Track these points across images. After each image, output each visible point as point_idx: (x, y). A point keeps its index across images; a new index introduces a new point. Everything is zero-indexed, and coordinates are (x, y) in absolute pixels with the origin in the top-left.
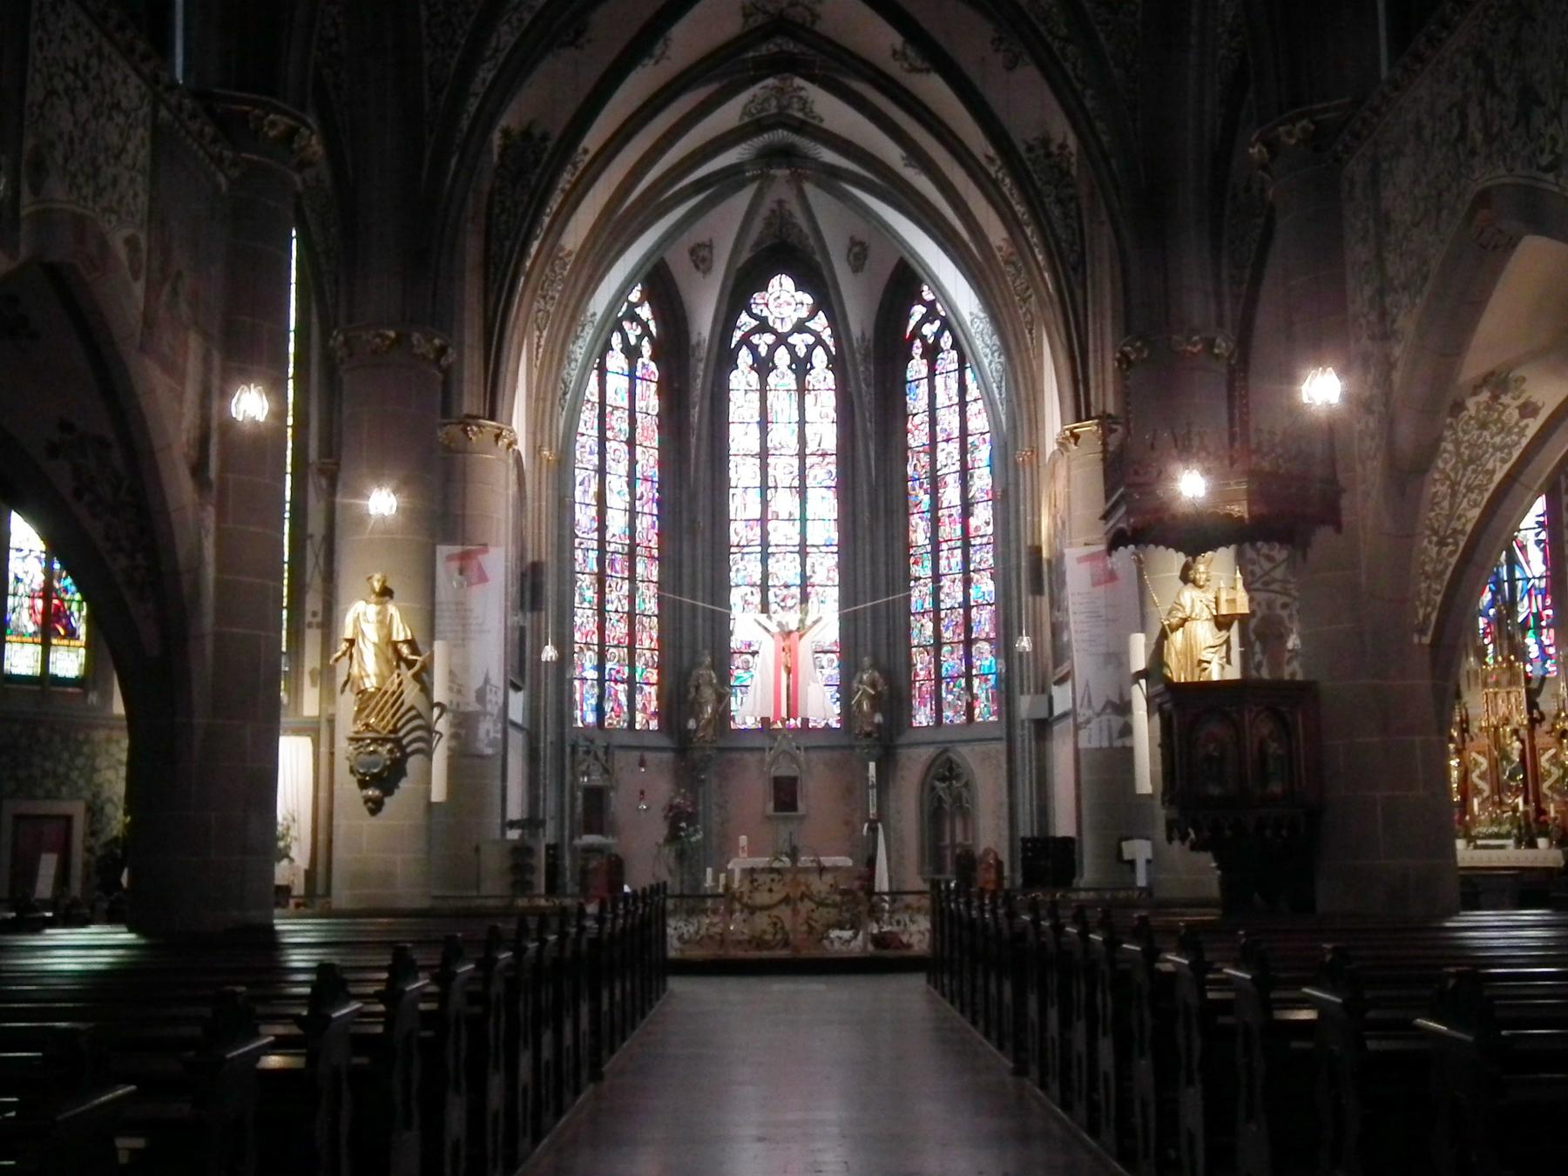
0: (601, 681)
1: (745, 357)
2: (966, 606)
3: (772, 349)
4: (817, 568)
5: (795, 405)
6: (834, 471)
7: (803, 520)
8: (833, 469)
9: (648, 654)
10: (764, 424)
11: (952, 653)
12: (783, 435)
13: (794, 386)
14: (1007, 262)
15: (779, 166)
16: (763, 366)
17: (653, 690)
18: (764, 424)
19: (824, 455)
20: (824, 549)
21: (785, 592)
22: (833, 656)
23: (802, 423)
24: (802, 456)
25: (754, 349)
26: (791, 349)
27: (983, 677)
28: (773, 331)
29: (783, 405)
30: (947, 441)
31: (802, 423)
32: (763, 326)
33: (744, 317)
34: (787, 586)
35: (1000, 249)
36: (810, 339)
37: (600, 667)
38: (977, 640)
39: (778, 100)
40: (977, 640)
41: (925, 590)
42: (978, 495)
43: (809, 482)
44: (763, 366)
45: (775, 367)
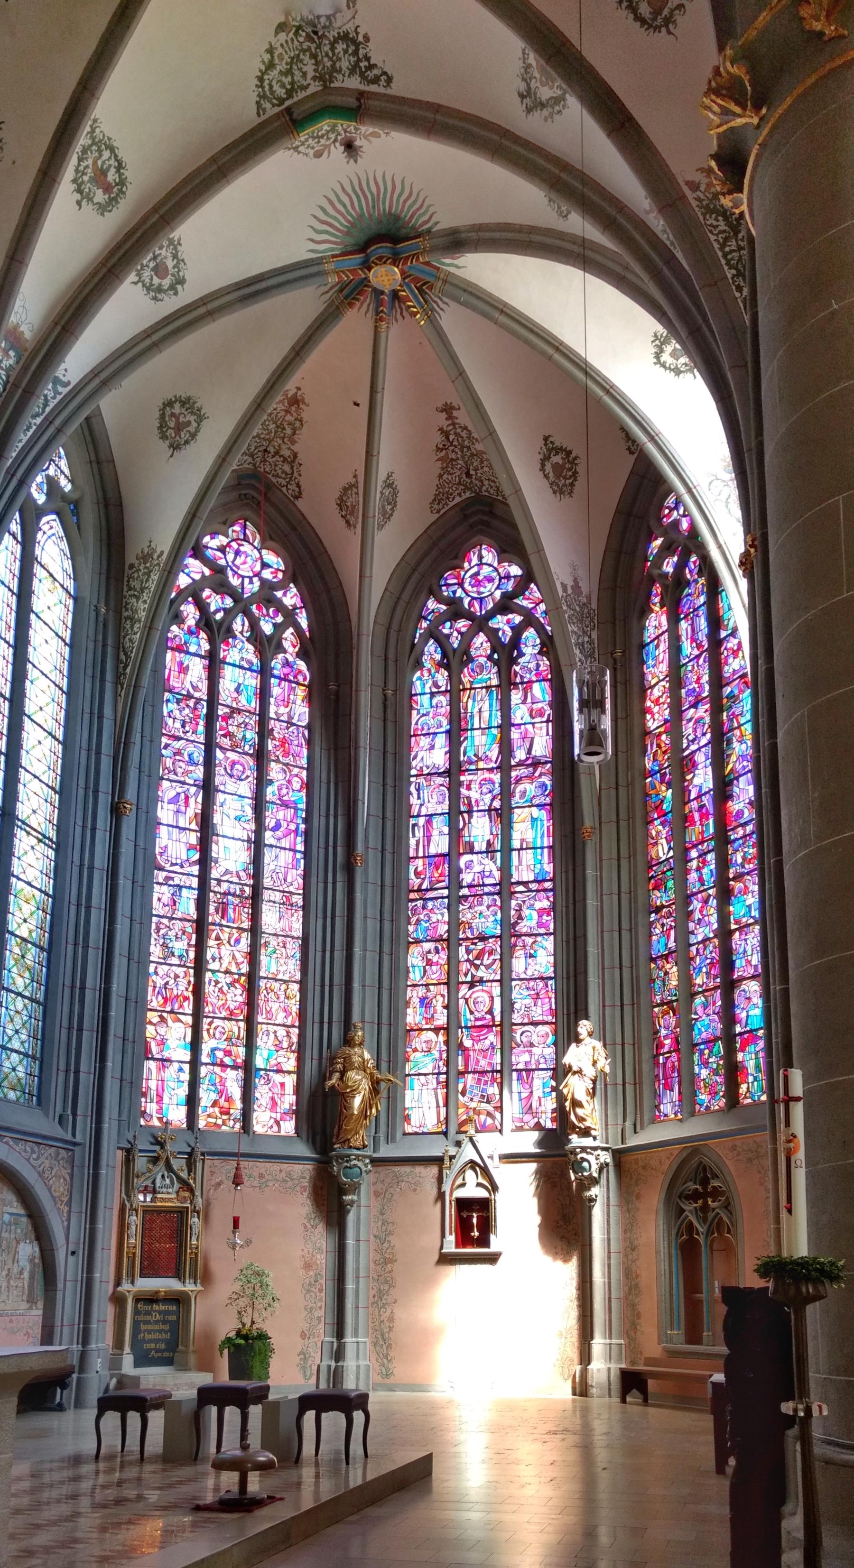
0: (195, 1064)
1: (432, 651)
2: (725, 934)
3: (467, 638)
4: (526, 912)
5: (496, 705)
6: (548, 783)
7: (507, 850)
8: (547, 780)
9: (281, 1032)
10: (456, 731)
11: (705, 1007)
12: (480, 743)
13: (495, 682)
14: (709, 210)
15: (381, 261)
16: (455, 660)
17: (290, 1081)
18: (456, 731)
19: (536, 763)
20: (533, 886)
21: (480, 945)
22: (547, 1029)
23: (506, 725)
24: (504, 767)
25: (442, 642)
26: (492, 635)
27: (750, 1037)
28: (469, 616)
29: (481, 708)
30: (695, 705)
31: (506, 725)
32: (456, 611)
33: (431, 604)
34: (483, 938)
35: (694, 186)
36: (517, 619)
37: (195, 1045)
38: (742, 979)
39: (314, 56)
40: (742, 979)
41: (669, 922)
42: (739, 767)
43: (516, 800)
44: (455, 660)
45: (471, 660)
